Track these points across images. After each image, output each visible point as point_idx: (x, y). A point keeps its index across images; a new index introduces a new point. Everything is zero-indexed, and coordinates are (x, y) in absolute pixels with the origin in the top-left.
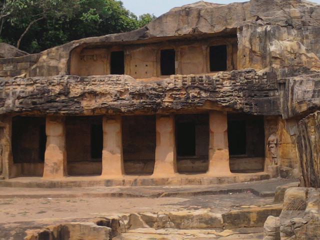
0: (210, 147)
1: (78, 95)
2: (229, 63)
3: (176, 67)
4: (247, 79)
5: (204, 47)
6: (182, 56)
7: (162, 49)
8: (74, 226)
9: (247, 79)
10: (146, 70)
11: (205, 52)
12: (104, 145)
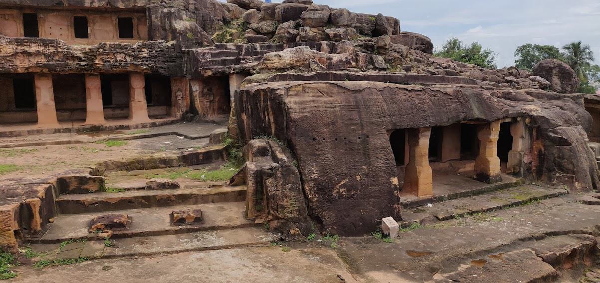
0: (132, 99)
1: (10, 55)
2: (135, 33)
3: (89, 31)
4: (160, 48)
5: (114, 18)
6: (94, 24)
7: (75, 15)
8: (70, 178)
9: (160, 48)
10: (60, 33)
11: (114, 22)
12: (38, 98)
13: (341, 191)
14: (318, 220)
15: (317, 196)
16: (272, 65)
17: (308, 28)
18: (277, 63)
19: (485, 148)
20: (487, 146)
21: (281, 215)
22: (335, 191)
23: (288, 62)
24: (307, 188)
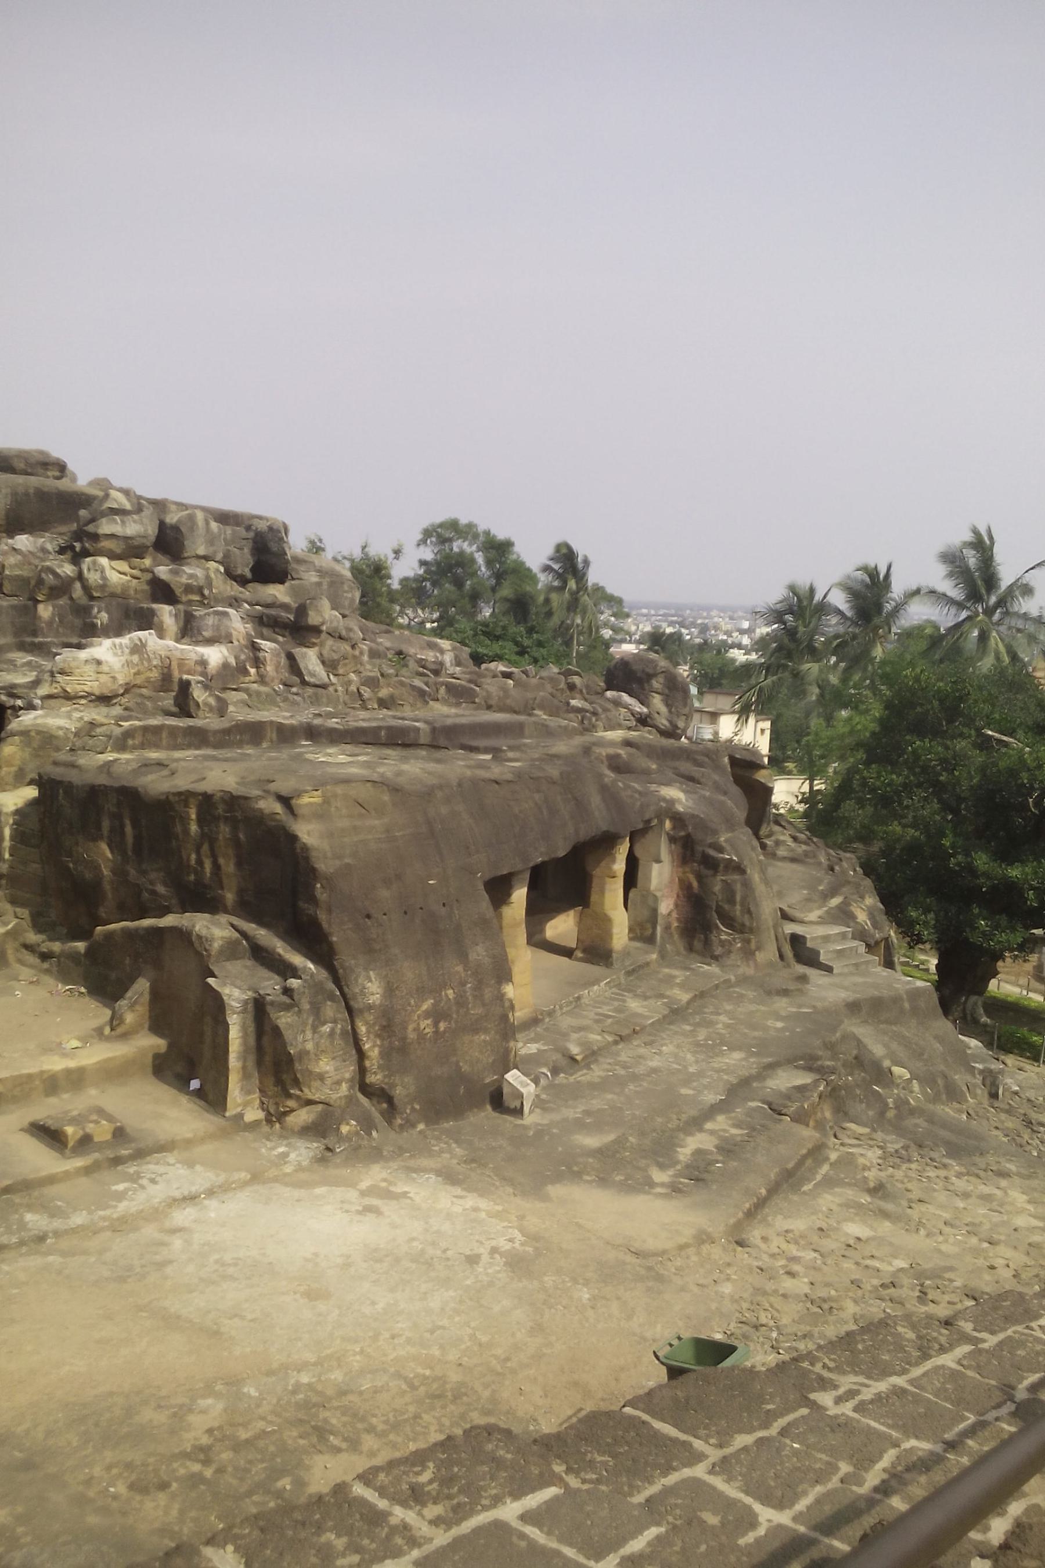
13: (422, 1027)
14: (382, 1095)
15: (378, 1043)
16: (79, 688)
17: (104, 561)
18: (90, 683)
19: (602, 892)
20: (607, 887)
21: (316, 1097)
22: (411, 1027)
23: (121, 679)
24: (362, 1029)
